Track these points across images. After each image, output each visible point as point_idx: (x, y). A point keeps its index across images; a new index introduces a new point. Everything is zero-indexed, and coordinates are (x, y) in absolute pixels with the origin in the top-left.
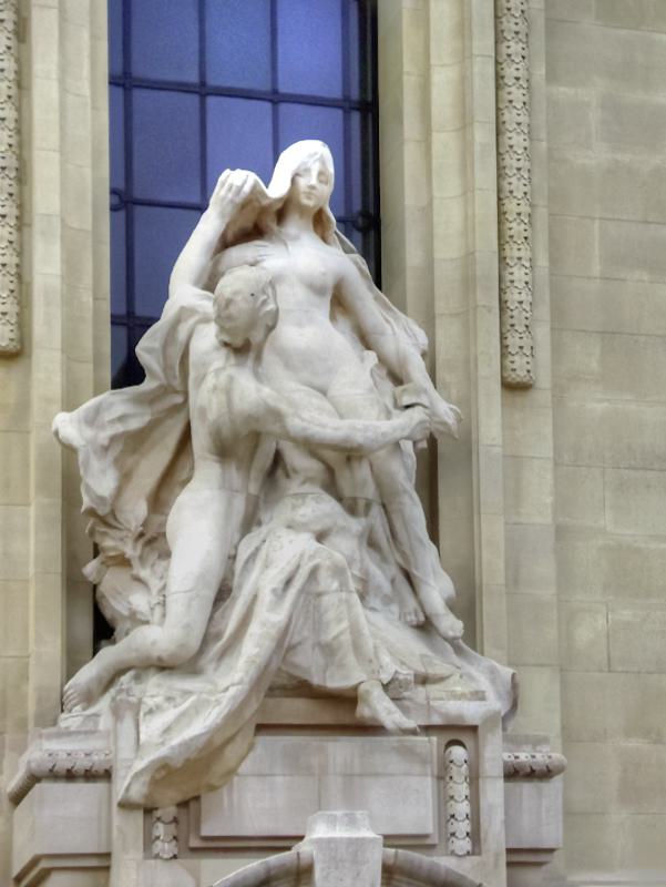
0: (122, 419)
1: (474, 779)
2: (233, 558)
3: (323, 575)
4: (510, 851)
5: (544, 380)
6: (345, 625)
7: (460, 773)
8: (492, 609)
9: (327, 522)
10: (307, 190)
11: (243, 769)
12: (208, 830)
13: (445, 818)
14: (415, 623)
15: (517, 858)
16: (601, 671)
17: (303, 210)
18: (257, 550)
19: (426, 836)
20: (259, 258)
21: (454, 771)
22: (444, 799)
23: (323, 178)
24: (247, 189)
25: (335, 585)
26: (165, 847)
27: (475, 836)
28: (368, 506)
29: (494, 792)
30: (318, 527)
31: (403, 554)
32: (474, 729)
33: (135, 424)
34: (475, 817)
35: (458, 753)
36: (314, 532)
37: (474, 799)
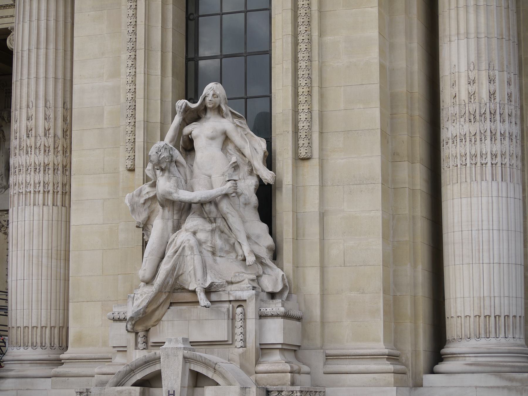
1: (244, 319)
3: (186, 249)
5: (316, 154)
6: (192, 267)
7: (238, 317)
9: (196, 228)
11: (163, 319)
18: (174, 239)
21: (237, 317)
23: (215, 96)
24: (183, 107)
25: (189, 253)
26: (141, 346)
28: (215, 219)
29: (251, 324)
30: (192, 230)
34: (244, 334)
35: (239, 310)
37: (244, 327)
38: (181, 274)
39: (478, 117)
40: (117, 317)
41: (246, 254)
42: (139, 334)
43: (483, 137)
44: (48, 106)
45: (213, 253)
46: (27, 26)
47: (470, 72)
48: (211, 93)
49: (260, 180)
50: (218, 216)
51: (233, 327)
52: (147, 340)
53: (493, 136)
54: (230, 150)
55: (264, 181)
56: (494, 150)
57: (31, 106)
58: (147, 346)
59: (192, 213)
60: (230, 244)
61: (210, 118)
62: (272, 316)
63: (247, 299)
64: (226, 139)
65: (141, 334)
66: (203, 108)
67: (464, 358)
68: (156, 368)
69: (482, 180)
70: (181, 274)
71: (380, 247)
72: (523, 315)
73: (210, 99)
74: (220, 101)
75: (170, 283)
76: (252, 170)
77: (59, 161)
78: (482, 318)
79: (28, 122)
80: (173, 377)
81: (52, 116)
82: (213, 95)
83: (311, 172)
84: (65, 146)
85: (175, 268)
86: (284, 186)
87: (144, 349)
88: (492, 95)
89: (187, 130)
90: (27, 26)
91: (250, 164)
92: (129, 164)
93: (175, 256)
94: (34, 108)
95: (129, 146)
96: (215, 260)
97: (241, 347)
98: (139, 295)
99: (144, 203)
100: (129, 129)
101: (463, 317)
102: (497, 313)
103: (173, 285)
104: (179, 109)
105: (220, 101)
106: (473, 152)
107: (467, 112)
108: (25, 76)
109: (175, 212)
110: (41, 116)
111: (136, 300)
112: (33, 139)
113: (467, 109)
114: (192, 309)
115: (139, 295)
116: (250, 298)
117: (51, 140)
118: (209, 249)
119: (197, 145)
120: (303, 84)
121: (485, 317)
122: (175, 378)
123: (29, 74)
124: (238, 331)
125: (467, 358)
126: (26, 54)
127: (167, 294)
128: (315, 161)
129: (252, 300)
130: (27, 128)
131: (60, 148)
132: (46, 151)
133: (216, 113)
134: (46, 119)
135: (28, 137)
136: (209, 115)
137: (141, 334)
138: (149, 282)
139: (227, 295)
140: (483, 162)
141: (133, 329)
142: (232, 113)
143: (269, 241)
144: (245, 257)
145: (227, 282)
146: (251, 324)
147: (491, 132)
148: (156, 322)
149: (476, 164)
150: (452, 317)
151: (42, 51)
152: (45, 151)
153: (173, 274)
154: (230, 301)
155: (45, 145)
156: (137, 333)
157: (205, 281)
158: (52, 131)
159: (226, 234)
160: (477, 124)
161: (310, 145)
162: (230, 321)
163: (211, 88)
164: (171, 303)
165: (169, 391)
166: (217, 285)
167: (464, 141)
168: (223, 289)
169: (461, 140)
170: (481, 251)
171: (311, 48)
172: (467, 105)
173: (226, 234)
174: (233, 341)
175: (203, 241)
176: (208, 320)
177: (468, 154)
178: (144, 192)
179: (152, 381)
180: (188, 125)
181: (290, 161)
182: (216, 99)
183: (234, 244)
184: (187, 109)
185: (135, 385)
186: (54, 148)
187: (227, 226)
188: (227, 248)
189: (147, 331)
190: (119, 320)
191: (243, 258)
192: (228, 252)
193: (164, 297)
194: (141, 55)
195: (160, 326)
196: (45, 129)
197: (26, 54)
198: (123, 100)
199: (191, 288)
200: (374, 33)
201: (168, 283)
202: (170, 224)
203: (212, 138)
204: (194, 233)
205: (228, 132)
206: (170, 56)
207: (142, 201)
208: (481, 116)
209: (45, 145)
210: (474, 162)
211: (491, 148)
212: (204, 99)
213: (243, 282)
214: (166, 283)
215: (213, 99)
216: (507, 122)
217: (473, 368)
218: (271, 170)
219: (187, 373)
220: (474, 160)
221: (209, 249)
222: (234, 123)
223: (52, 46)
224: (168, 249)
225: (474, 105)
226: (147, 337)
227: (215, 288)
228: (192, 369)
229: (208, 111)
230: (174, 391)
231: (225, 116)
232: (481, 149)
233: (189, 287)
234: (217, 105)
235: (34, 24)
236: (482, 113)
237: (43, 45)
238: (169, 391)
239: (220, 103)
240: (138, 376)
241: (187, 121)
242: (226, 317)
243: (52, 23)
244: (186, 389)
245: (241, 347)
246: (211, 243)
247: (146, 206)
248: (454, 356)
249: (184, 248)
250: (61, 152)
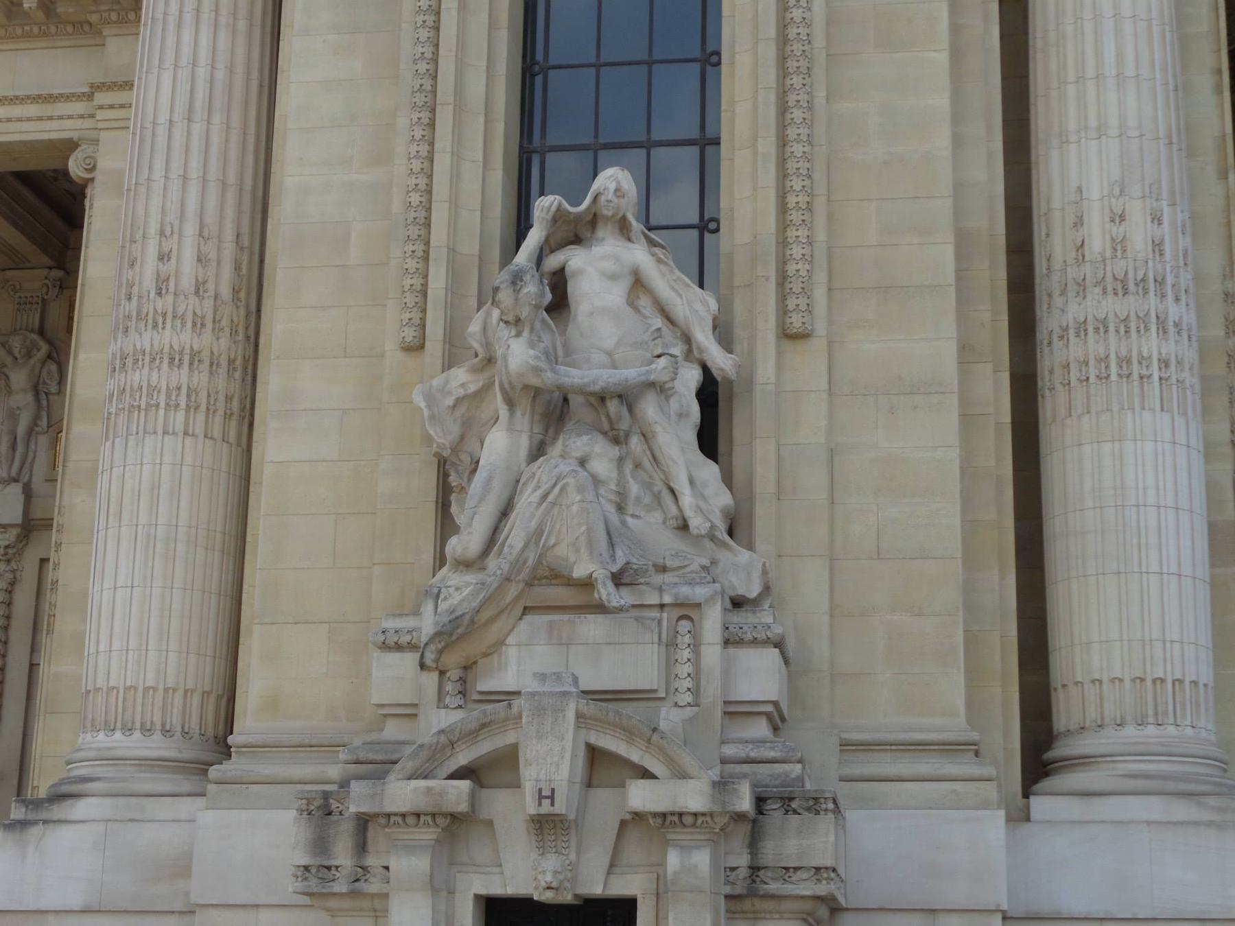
0: (462, 385)
1: (696, 646)
2: (518, 482)
4: (725, 702)
5: (821, 328)
6: (584, 528)
8: (764, 514)
12: (483, 686)
13: (669, 675)
15: (732, 709)
17: (607, 219)
19: (655, 691)
22: (670, 663)
24: (554, 208)
27: (696, 691)
28: (627, 435)
29: (712, 653)
31: (663, 471)
32: (699, 605)
33: (472, 388)
35: (685, 625)
37: (696, 661)
38: (554, 546)
39: (1132, 287)
40: (392, 639)
41: (689, 513)
42: (448, 675)
43: (1142, 326)
44: (206, 234)
45: (620, 508)
46: (167, 78)
47: (1113, 200)
48: (612, 186)
49: (706, 369)
53: (1161, 322)
55: (715, 372)
56: (1164, 351)
57: (168, 232)
58: (465, 702)
60: (653, 493)
61: (603, 239)
62: (755, 642)
63: (702, 601)
64: (638, 283)
67: (1111, 765)
68: (510, 738)
69: (1143, 409)
70: (554, 546)
71: (957, 521)
72: (1211, 684)
73: (610, 197)
75: (530, 562)
76: (690, 351)
77: (222, 347)
78: (1149, 682)
79: (161, 265)
81: (213, 255)
82: (617, 190)
83: (808, 365)
84: (235, 319)
85: (542, 531)
86: (758, 389)
87: (460, 707)
88: (1157, 246)
89: (553, 262)
90: (167, 78)
91: (687, 339)
92: (410, 334)
94: (176, 236)
95: (411, 299)
96: (624, 523)
97: (689, 705)
98: (451, 590)
99: (454, 407)
101: (1105, 680)
102: (1178, 676)
103: (535, 568)
104: (543, 215)
106: (1124, 352)
107: (1109, 275)
108: (158, 174)
109: (537, 418)
110: (189, 254)
111: (446, 598)
112: (170, 299)
113: (1109, 268)
115: (451, 590)
116: (710, 600)
117: (208, 304)
118: (613, 497)
119: (575, 289)
120: (797, 187)
121: (1154, 681)
122: (555, 759)
123: (167, 169)
125: (1119, 765)
126: (162, 132)
127: (521, 586)
128: (818, 344)
130: (158, 275)
131: (225, 322)
132: (198, 324)
134: (199, 260)
135: (159, 294)
136: (600, 233)
137: (454, 674)
140: (1144, 372)
141: (437, 661)
142: (646, 236)
143: (722, 499)
144: (685, 520)
145: (655, 566)
146: (712, 653)
147: (1158, 317)
148: (494, 645)
149: (1129, 376)
150: (1077, 683)
151: (197, 128)
152: (194, 324)
153: (537, 544)
155: (195, 313)
156: (442, 673)
157: (613, 557)
158: (211, 286)
159: (645, 471)
160: (1131, 298)
161: (809, 309)
162: (663, 648)
164: (525, 608)
166: (636, 570)
167: (1102, 330)
169: (1097, 330)
170: (1143, 547)
171: (812, 121)
172: (1108, 262)
173: (645, 471)
174: (667, 692)
177: (1113, 356)
178: (454, 384)
180: (552, 251)
181: (771, 338)
183: (660, 492)
184: (558, 218)
185: (452, 776)
186: (214, 321)
187: (648, 453)
188: (647, 499)
190: (398, 647)
191: (680, 522)
192: (649, 509)
193: (513, 591)
194: (445, 116)
195: (500, 656)
196: (197, 280)
197: (162, 132)
198: (397, 205)
199: (579, 572)
200: (941, 101)
201: (525, 562)
202: (524, 443)
203: (613, 277)
204: (582, 462)
206: (499, 128)
207: (450, 401)
208: (1137, 285)
209: (195, 313)
210: (1125, 371)
211: (1159, 348)
212: (596, 198)
215: (616, 200)
216: (1183, 302)
217: (1130, 784)
218: (730, 351)
219: (582, 752)
220: (1125, 368)
221: (613, 497)
222: (653, 255)
223: (217, 119)
224: (521, 492)
225: (1123, 264)
228: (593, 741)
229: (600, 225)
230: (553, 790)
231: (633, 238)
232: (1140, 348)
234: (620, 215)
235: (184, 75)
236: (1139, 278)
237: (199, 115)
238: (540, 790)
240: (463, 758)
242: (656, 639)
243: (221, 74)
244: (578, 786)
246: (618, 485)
247: (459, 412)
248: (1084, 761)
249: (563, 489)
250: (227, 331)
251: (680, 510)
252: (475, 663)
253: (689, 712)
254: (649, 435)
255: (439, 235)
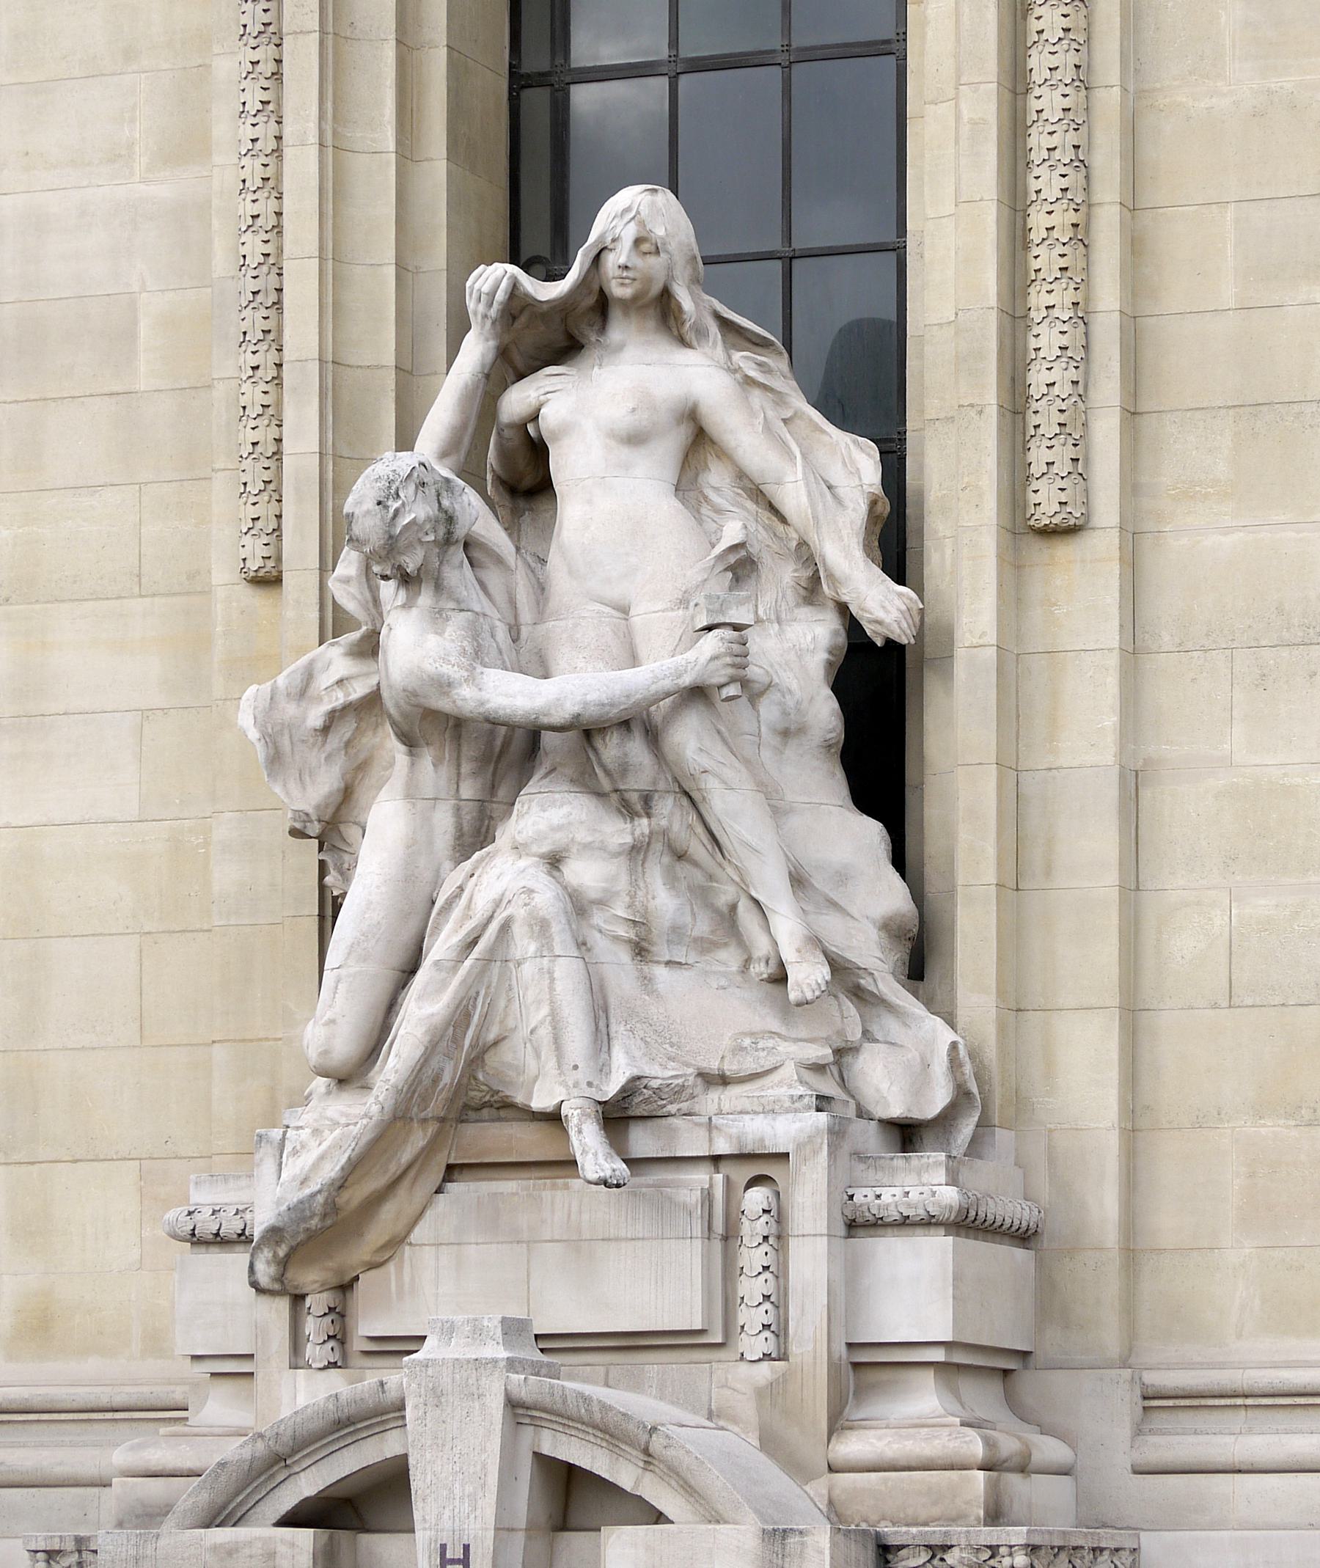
3: (518, 930)
6: (545, 1010)
7: (754, 1228)
9: (560, 838)
10: (618, 272)
11: (416, 1236)
14: (765, 976)
16: (1215, 1006)
18: (461, 888)
20: (542, 398)
21: (746, 1227)
23: (645, 247)
25: (532, 948)
26: (316, 1352)
28: (647, 799)
29: (811, 1260)
30: (545, 848)
34: (778, 1301)
35: (757, 1198)
36: (542, 856)
37: (778, 1270)
38: (496, 1043)
40: (207, 1225)
41: (788, 955)
42: (308, 1301)
45: (640, 950)
48: (629, 233)
50: (661, 786)
51: (730, 1272)
52: (344, 1330)
54: (717, 489)
58: (344, 1355)
59: (542, 771)
60: (716, 911)
61: (621, 348)
64: (698, 440)
65: (317, 1302)
66: (591, 300)
70: (496, 1043)
73: (622, 260)
74: (670, 268)
75: (446, 1078)
76: (815, 579)
80: (462, 1488)
82: (638, 242)
85: (468, 1016)
86: (960, 653)
87: (333, 1365)
89: (517, 400)
91: (805, 554)
92: (255, 552)
93: (468, 963)
95: (255, 474)
97: (767, 1357)
99: (326, 730)
100: (254, 395)
103: (460, 1088)
104: (481, 308)
105: (670, 268)
109: (466, 768)
111: (295, 1152)
114: (547, 1195)
118: (622, 931)
124: (752, 1287)
127: (432, 1128)
129: (815, 1152)
133: (651, 324)
136: (618, 331)
137: (317, 1302)
138: (348, 1077)
139: (703, 1133)
141: (280, 1278)
142: (725, 324)
144: (782, 965)
148: (384, 1247)
153: (457, 1041)
154: (716, 1160)
156: (298, 1299)
157: (604, 1070)
159: (696, 864)
162: (717, 1246)
163: (627, 210)
164: (450, 1168)
165: (443, 1548)
168: (685, 1106)
175: (593, 895)
176: (617, 1239)
178: (324, 680)
179: (368, 1503)
180: (521, 376)
181: (988, 543)
182: (652, 260)
183: (733, 908)
185: (291, 1520)
187: (700, 830)
188: (703, 926)
189: (345, 1287)
190: (219, 1241)
192: (706, 946)
193: (418, 1139)
199: (540, 1102)
201: (436, 1080)
202: (444, 821)
203: (635, 439)
204: (554, 861)
205: (704, 410)
207: (315, 717)
213: (775, 1077)
214: (427, 1082)
215: (638, 262)
218: (901, 580)
221: (622, 931)
222: (733, 370)
224: (437, 929)
226: (343, 1316)
227: (646, 1101)
228: (546, 1450)
230: (466, 1548)
231: (691, 336)
233: (530, 1095)
234: (656, 289)
238: (443, 1548)
239: (670, 277)
240: (308, 1484)
241: (519, 362)
242: (698, 1229)
244: (520, 1538)
245: (767, 1357)
247: (335, 741)
249: (506, 927)
251: (775, 943)
252: (357, 1278)
253: (765, 1371)
254: (694, 795)
255: (302, 334)
